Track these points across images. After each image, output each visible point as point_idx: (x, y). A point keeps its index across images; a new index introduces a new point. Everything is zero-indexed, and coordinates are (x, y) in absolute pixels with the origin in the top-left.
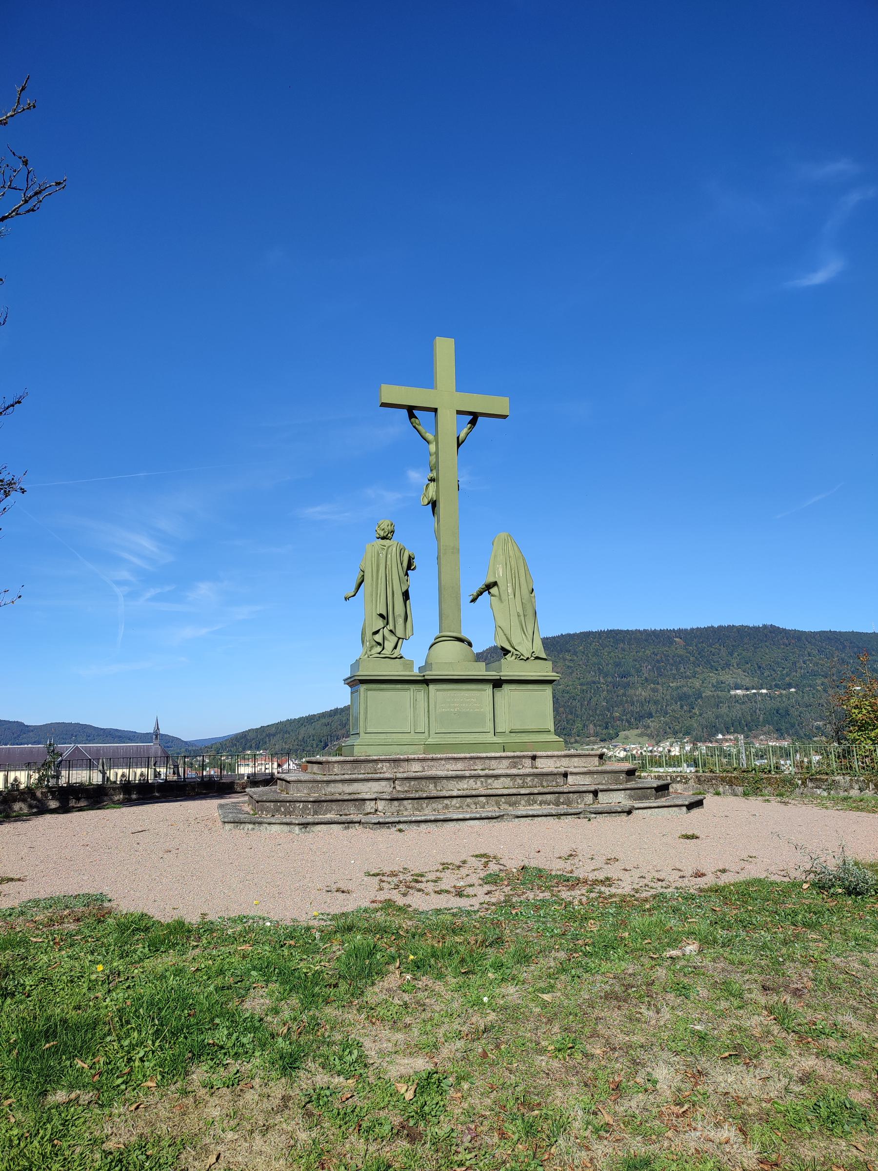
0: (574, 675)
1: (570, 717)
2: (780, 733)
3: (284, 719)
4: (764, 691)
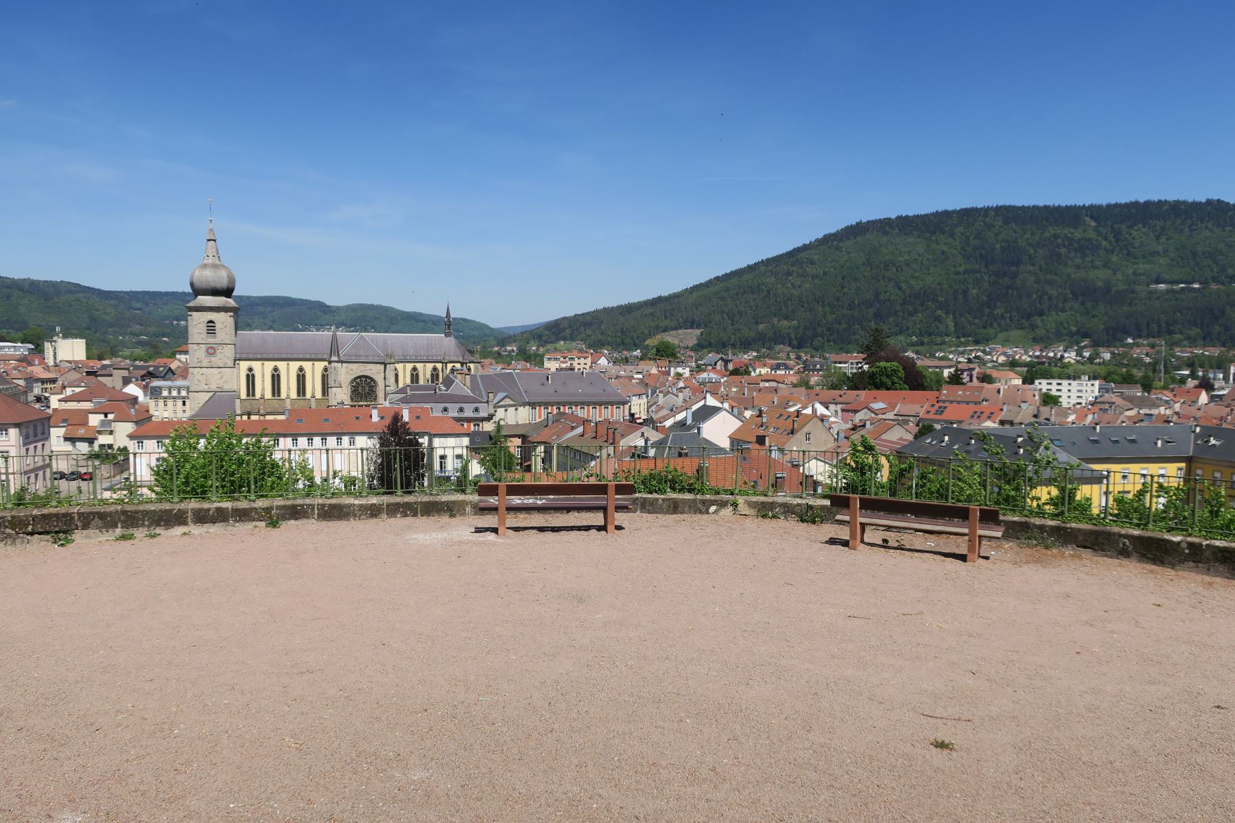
2: (1207, 339)
3: (600, 307)
4: (1196, 286)
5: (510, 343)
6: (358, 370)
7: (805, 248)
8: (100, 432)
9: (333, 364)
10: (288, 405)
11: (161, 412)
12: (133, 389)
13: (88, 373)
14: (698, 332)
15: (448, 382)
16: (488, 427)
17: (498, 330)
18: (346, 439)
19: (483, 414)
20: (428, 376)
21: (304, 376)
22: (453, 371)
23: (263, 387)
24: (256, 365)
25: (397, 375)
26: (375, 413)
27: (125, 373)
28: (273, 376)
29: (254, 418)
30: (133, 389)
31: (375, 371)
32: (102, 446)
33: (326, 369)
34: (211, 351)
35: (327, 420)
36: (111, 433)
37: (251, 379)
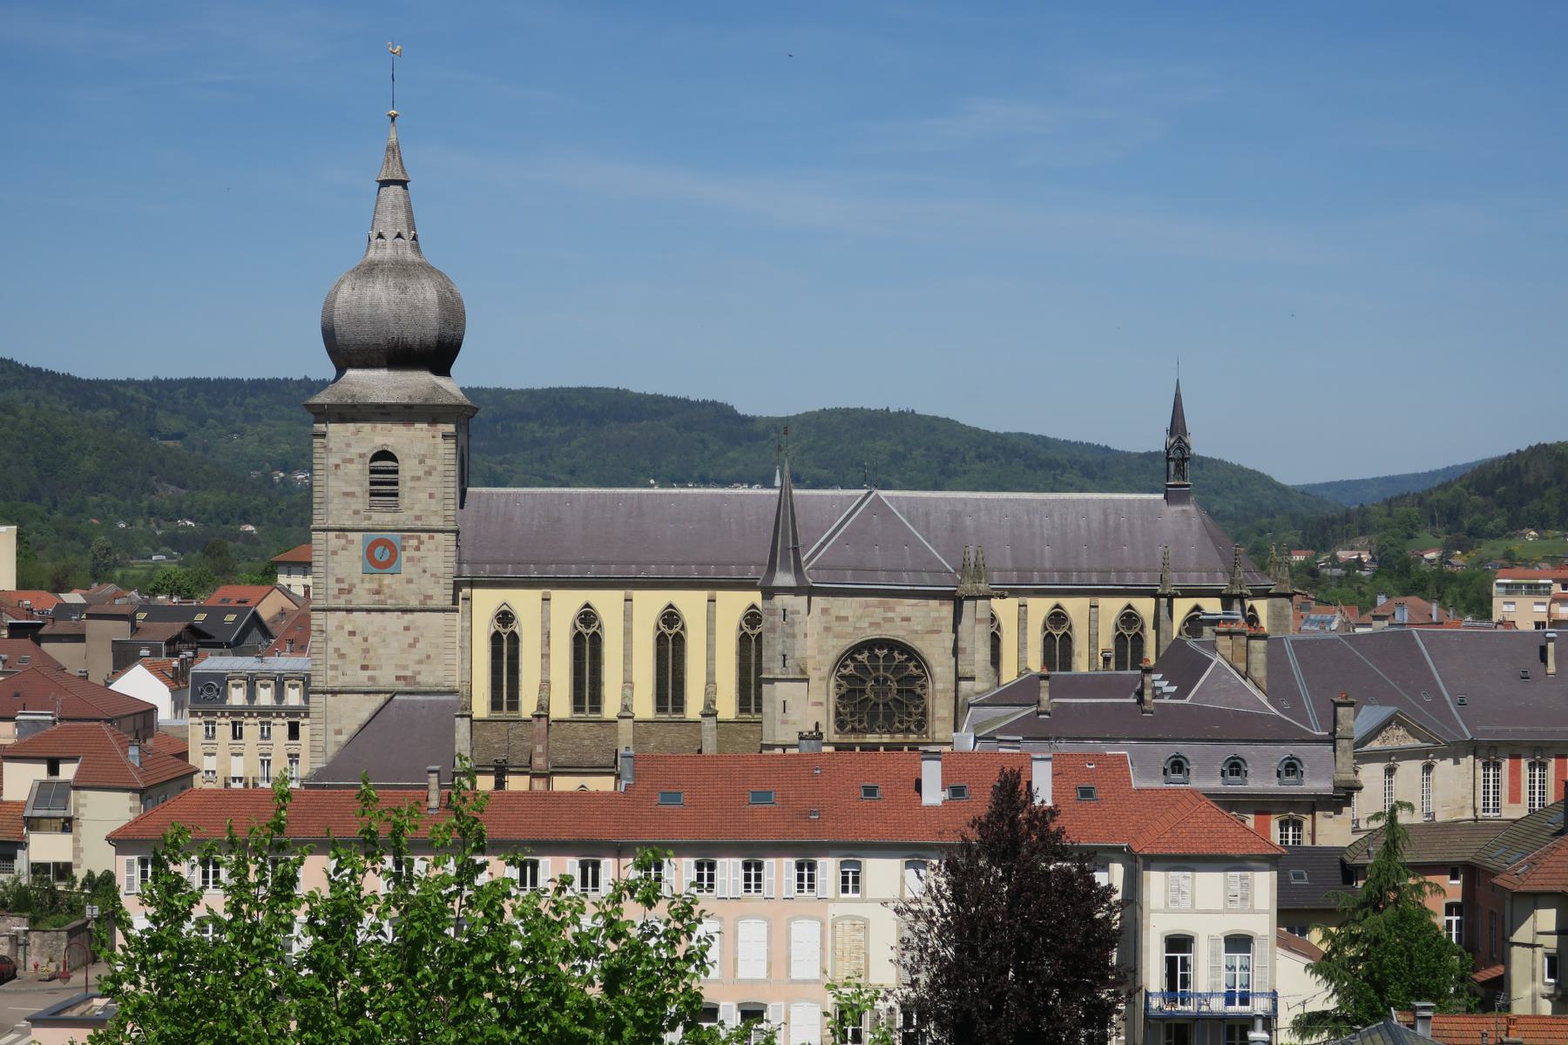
5: (1345, 539)
6: (861, 619)
8: (34, 824)
9: (781, 600)
10: (625, 737)
11: (225, 759)
12: (141, 684)
13: (16, 631)
15: (1184, 664)
16: (1332, 832)
17: (1305, 492)
18: (828, 868)
19: (1316, 784)
20: (1106, 641)
21: (679, 640)
22: (1195, 622)
23: (546, 678)
24: (524, 602)
25: (995, 640)
26: (931, 772)
27: (121, 630)
28: (578, 639)
29: (516, 783)
30: (141, 684)
31: (918, 622)
32: (38, 869)
33: (752, 617)
34: (382, 555)
35: (762, 797)
36: (67, 825)
37: (505, 649)
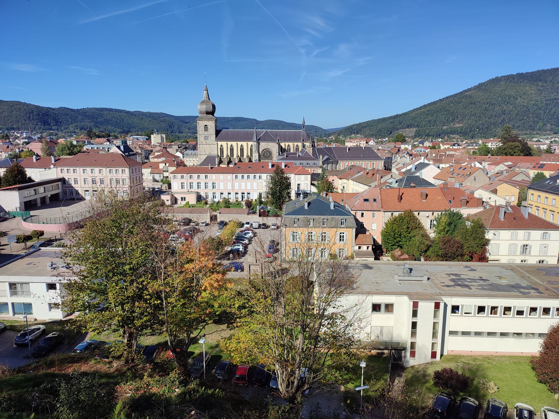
0: (543, 95)
1: (535, 119)
7: (469, 90)
12: (179, 154)
14: (415, 129)
30: (179, 154)
